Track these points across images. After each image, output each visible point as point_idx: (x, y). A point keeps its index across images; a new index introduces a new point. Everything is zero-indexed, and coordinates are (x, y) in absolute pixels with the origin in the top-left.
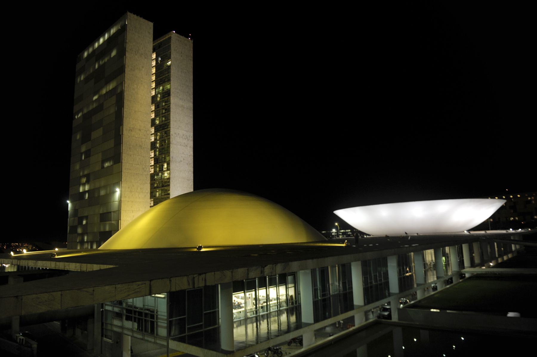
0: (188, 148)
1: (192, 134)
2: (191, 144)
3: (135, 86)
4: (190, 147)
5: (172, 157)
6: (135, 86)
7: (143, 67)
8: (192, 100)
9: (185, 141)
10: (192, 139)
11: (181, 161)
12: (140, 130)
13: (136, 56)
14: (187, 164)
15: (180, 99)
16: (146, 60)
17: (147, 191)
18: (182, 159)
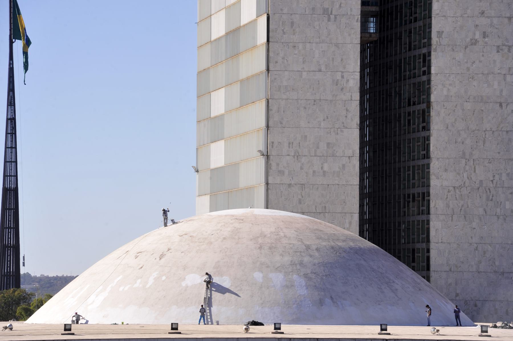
5: (440, 34)
11: (474, 42)
17: (349, 153)
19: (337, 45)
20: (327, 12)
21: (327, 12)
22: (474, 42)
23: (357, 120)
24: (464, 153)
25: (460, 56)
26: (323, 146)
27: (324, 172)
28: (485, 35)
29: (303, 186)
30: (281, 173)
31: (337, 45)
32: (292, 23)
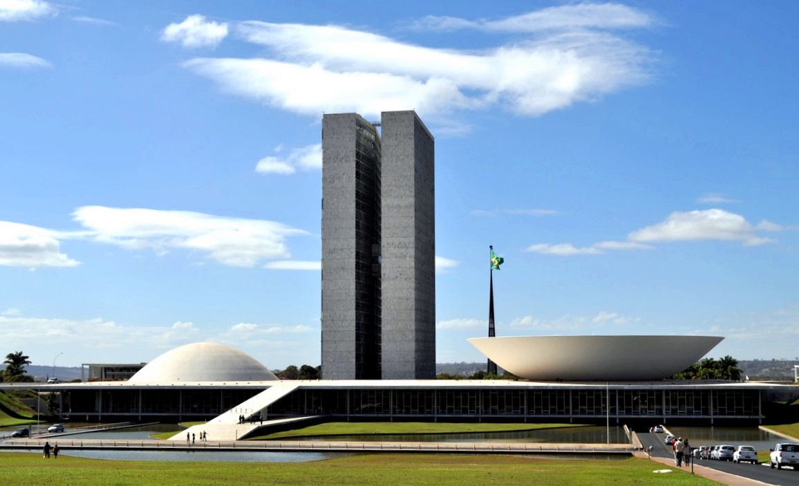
0: (408, 259)
1: (413, 239)
2: (412, 252)
3: (335, 200)
4: (410, 257)
5: (384, 274)
6: (335, 200)
7: (344, 174)
8: (413, 194)
9: (403, 251)
10: (412, 245)
11: (397, 277)
12: (342, 250)
13: (335, 164)
14: (406, 279)
15: (395, 197)
16: (347, 164)
17: (352, 319)
18: (398, 274)
19: (347, 280)
20: (343, 268)
21: (343, 268)
22: (397, 277)
23: (354, 306)
24: (394, 318)
25: (392, 282)
26: (342, 316)
27: (343, 326)
28: (401, 274)
29: (335, 331)
30: (327, 327)
31: (347, 280)
32: (330, 273)
